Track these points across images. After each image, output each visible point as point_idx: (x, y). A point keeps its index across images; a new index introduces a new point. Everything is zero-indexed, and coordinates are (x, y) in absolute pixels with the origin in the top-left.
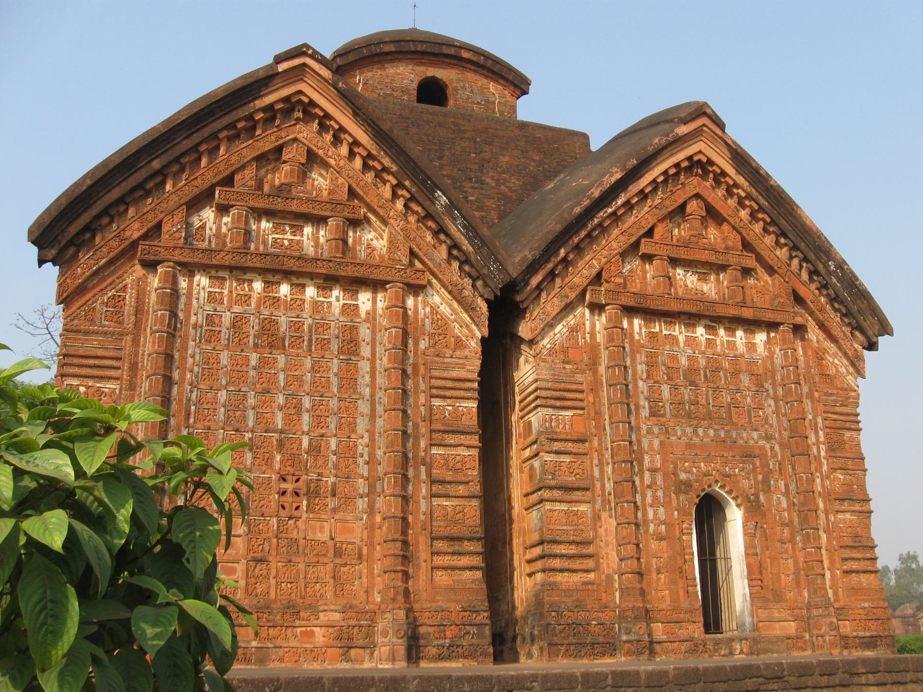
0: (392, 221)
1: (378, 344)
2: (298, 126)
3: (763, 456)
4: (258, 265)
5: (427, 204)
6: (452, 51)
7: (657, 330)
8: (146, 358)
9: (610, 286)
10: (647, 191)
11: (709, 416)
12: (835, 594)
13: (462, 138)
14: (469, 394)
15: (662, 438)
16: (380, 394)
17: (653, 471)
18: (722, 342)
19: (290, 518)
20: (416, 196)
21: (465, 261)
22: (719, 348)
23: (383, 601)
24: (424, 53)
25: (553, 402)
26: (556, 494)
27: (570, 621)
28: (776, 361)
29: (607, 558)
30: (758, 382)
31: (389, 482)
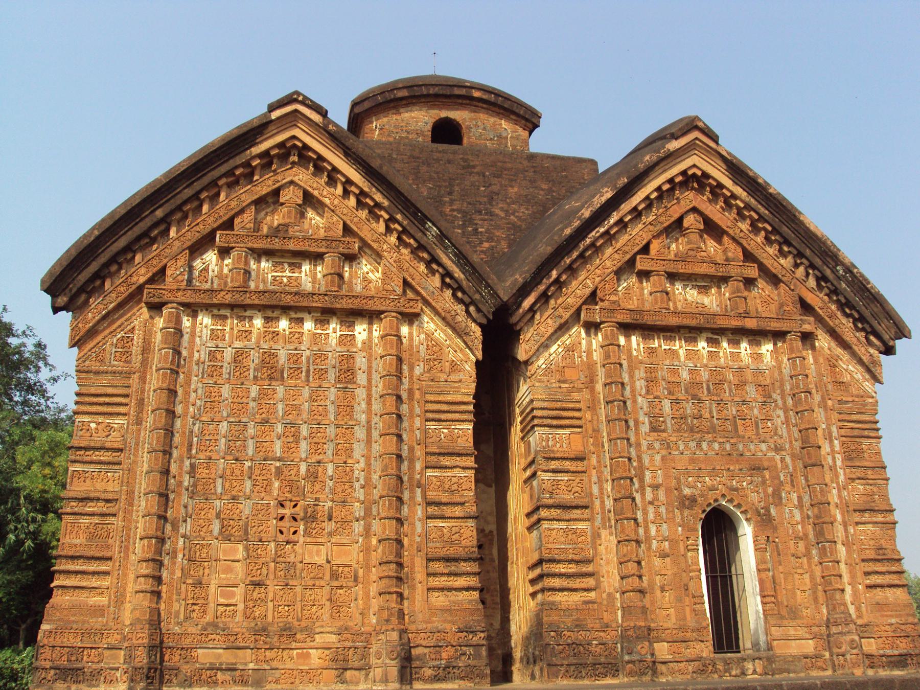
0: (385, 254)
1: (373, 371)
2: (294, 170)
3: (772, 468)
4: (256, 302)
5: (419, 235)
6: (463, 92)
7: (657, 345)
8: (151, 393)
9: (606, 304)
10: (640, 208)
11: (713, 429)
12: (858, 609)
13: (471, 174)
14: (465, 417)
15: (664, 452)
16: (376, 419)
17: (655, 487)
18: (725, 354)
19: (288, 542)
20: (408, 228)
21: (457, 288)
22: (722, 360)
23: (378, 621)
24: (436, 96)
25: (549, 421)
26: (554, 513)
27: (569, 641)
28: (784, 371)
29: (608, 576)
30: (766, 391)
31: (384, 504)
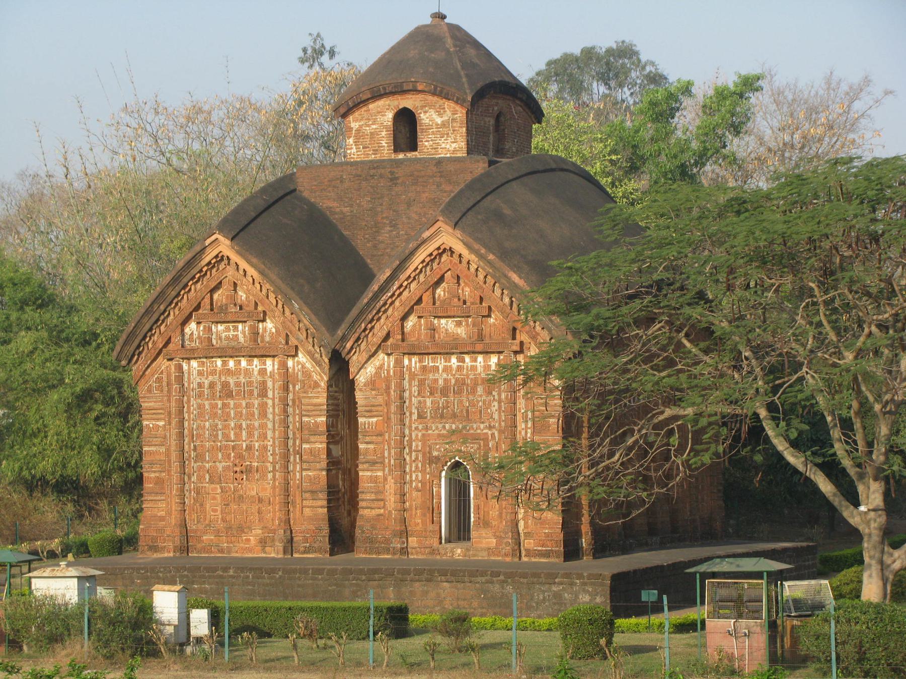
11: (454, 416)
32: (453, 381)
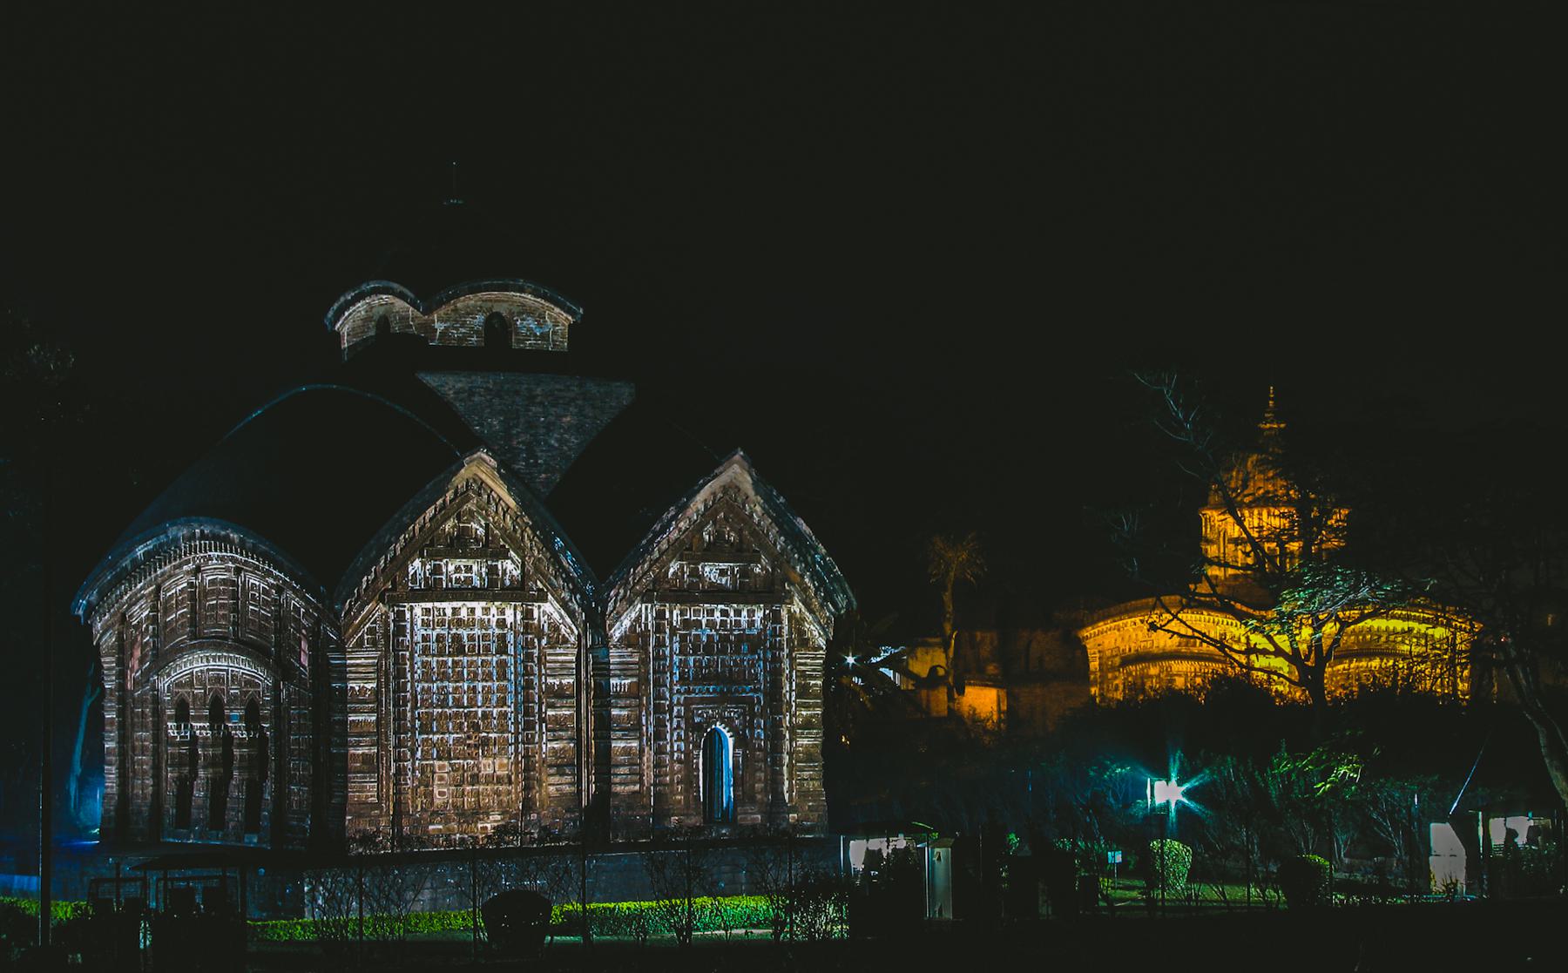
30: (753, 651)
32: (717, 638)
